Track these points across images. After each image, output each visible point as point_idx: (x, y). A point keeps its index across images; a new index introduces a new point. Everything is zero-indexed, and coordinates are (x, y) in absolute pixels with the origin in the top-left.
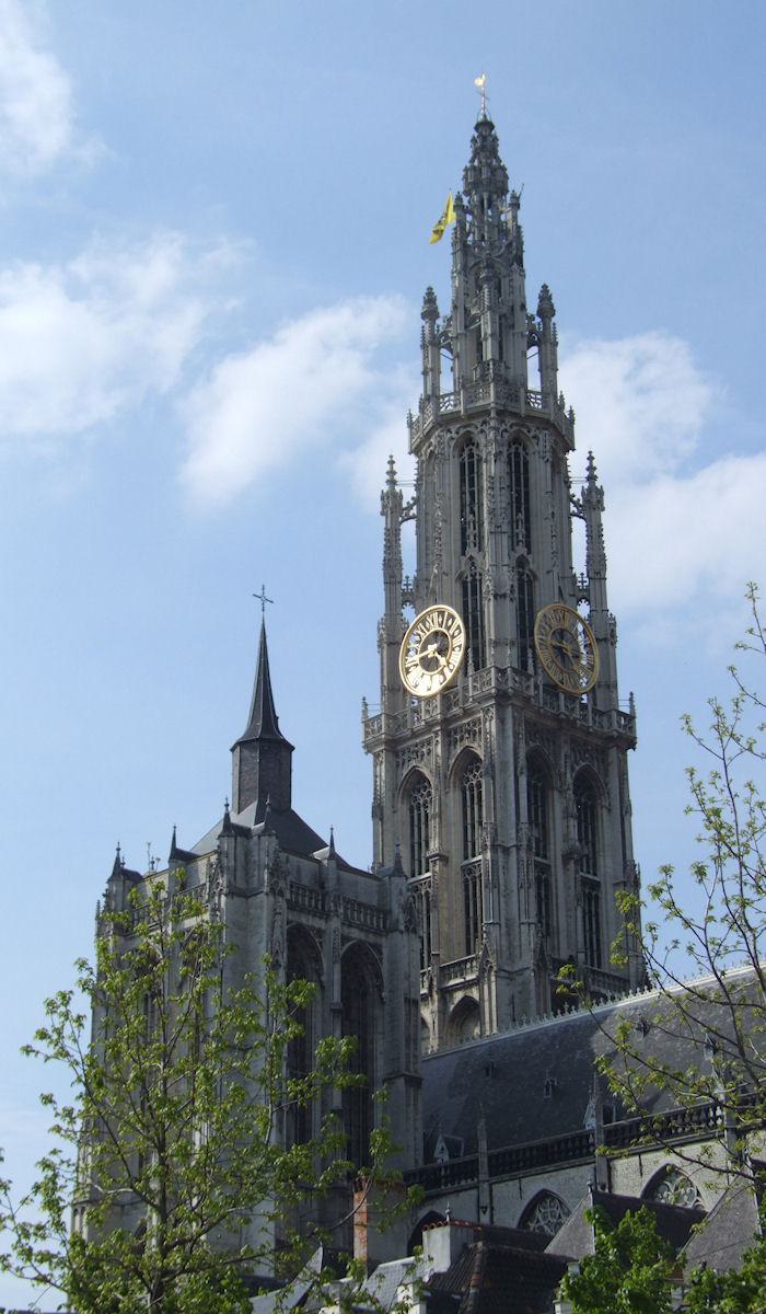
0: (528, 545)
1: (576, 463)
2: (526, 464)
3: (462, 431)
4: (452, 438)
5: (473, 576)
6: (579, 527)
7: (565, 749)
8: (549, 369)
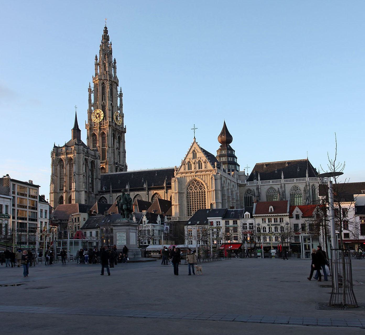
0: (112, 101)
3: (103, 82)
5: (104, 105)
7: (117, 133)
8: (115, 72)
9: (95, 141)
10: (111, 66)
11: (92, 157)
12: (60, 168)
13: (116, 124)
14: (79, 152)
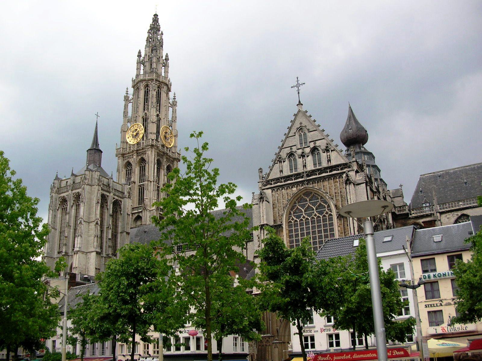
0: (159, 112)
1: (171, 95)
2: (160, 93)
3: (146, 83)
5: (146, 117)
8: (166, 72)
9: (129, 174)
10: (160, 62)
11: (117, 194)
12: (62, 214)
13: (163, 146)
14: (91, 182)
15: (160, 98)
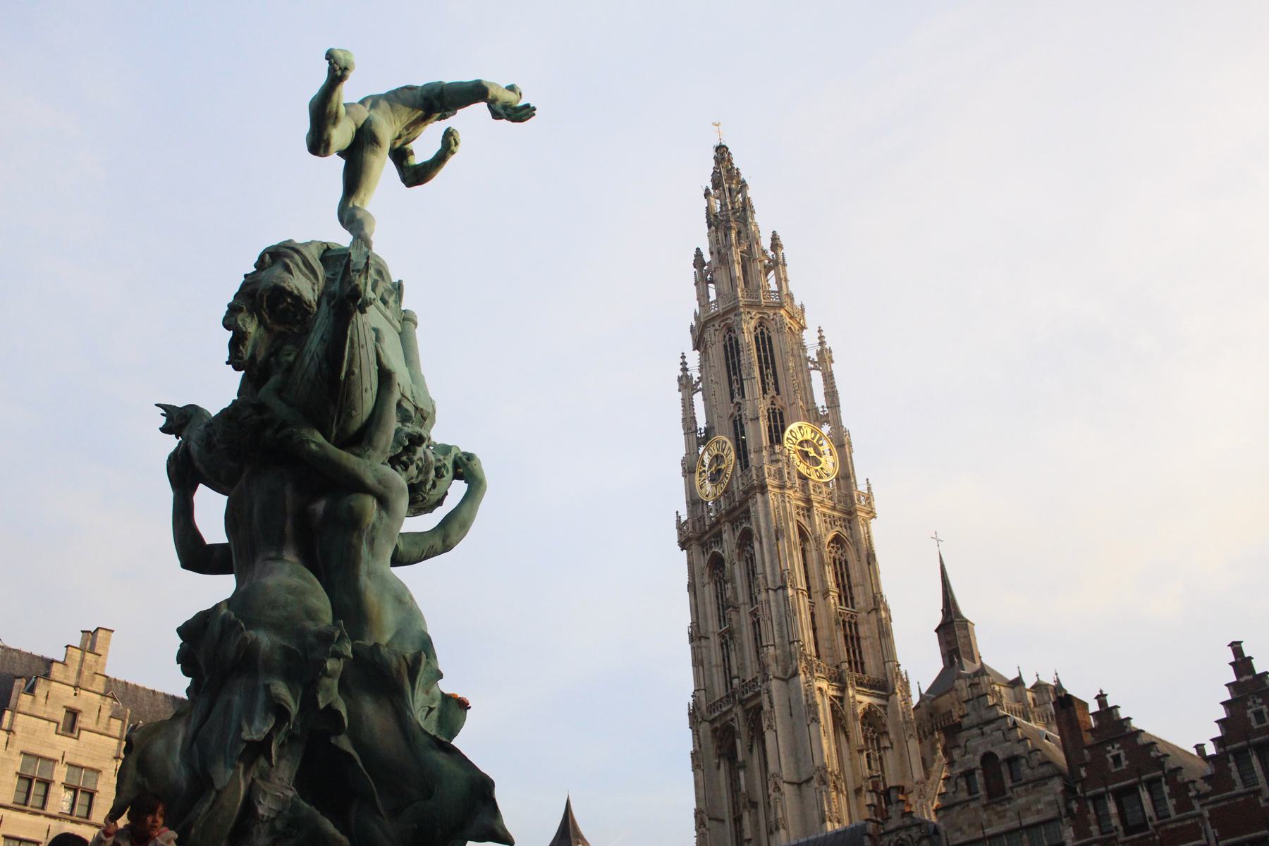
0: (777, 390)
1: (810, 339)
2: (769, 338)
3: (722, 324)
4: (716, 330)
5: (740, 415)
6: (817, 378)
15: (771, 351)
